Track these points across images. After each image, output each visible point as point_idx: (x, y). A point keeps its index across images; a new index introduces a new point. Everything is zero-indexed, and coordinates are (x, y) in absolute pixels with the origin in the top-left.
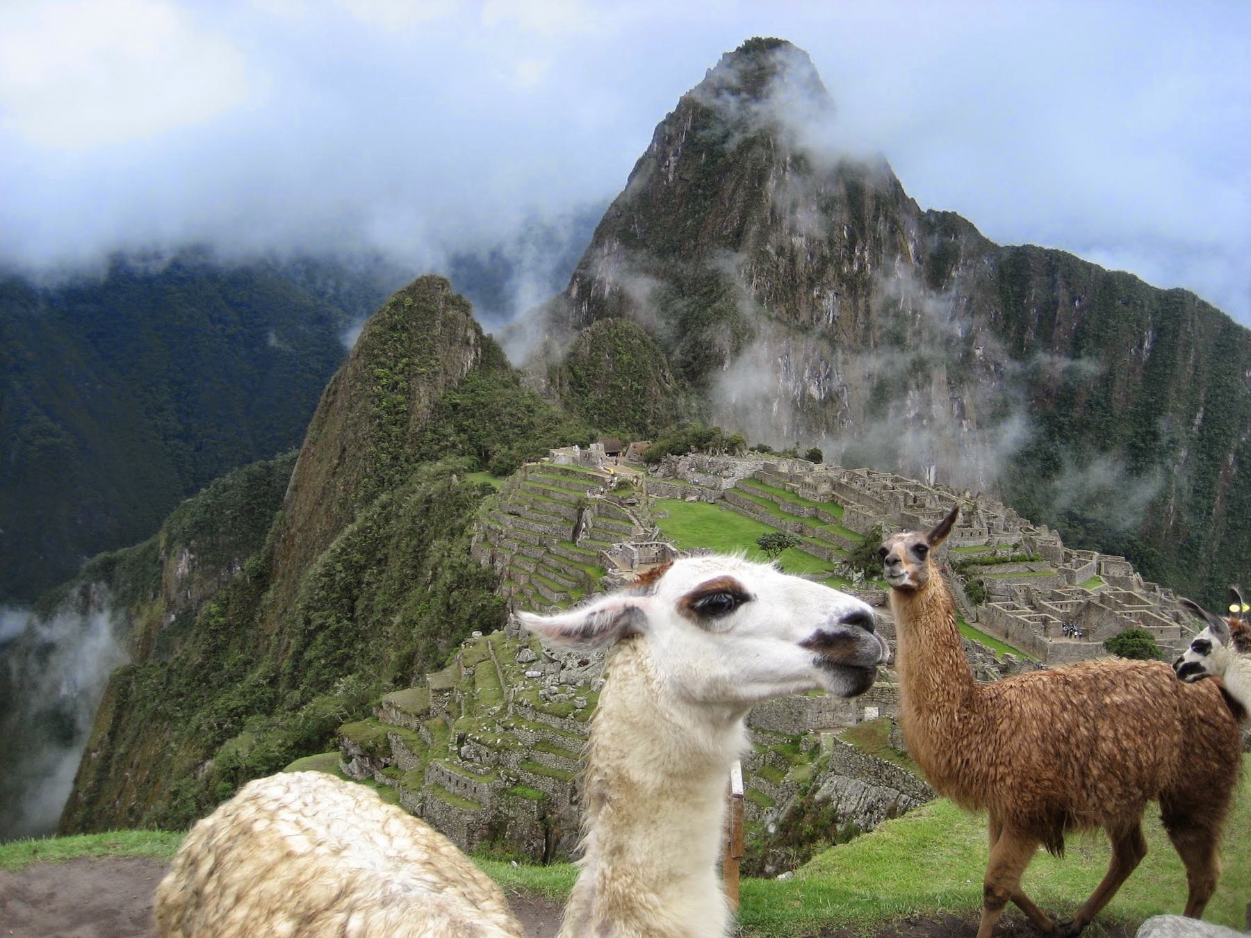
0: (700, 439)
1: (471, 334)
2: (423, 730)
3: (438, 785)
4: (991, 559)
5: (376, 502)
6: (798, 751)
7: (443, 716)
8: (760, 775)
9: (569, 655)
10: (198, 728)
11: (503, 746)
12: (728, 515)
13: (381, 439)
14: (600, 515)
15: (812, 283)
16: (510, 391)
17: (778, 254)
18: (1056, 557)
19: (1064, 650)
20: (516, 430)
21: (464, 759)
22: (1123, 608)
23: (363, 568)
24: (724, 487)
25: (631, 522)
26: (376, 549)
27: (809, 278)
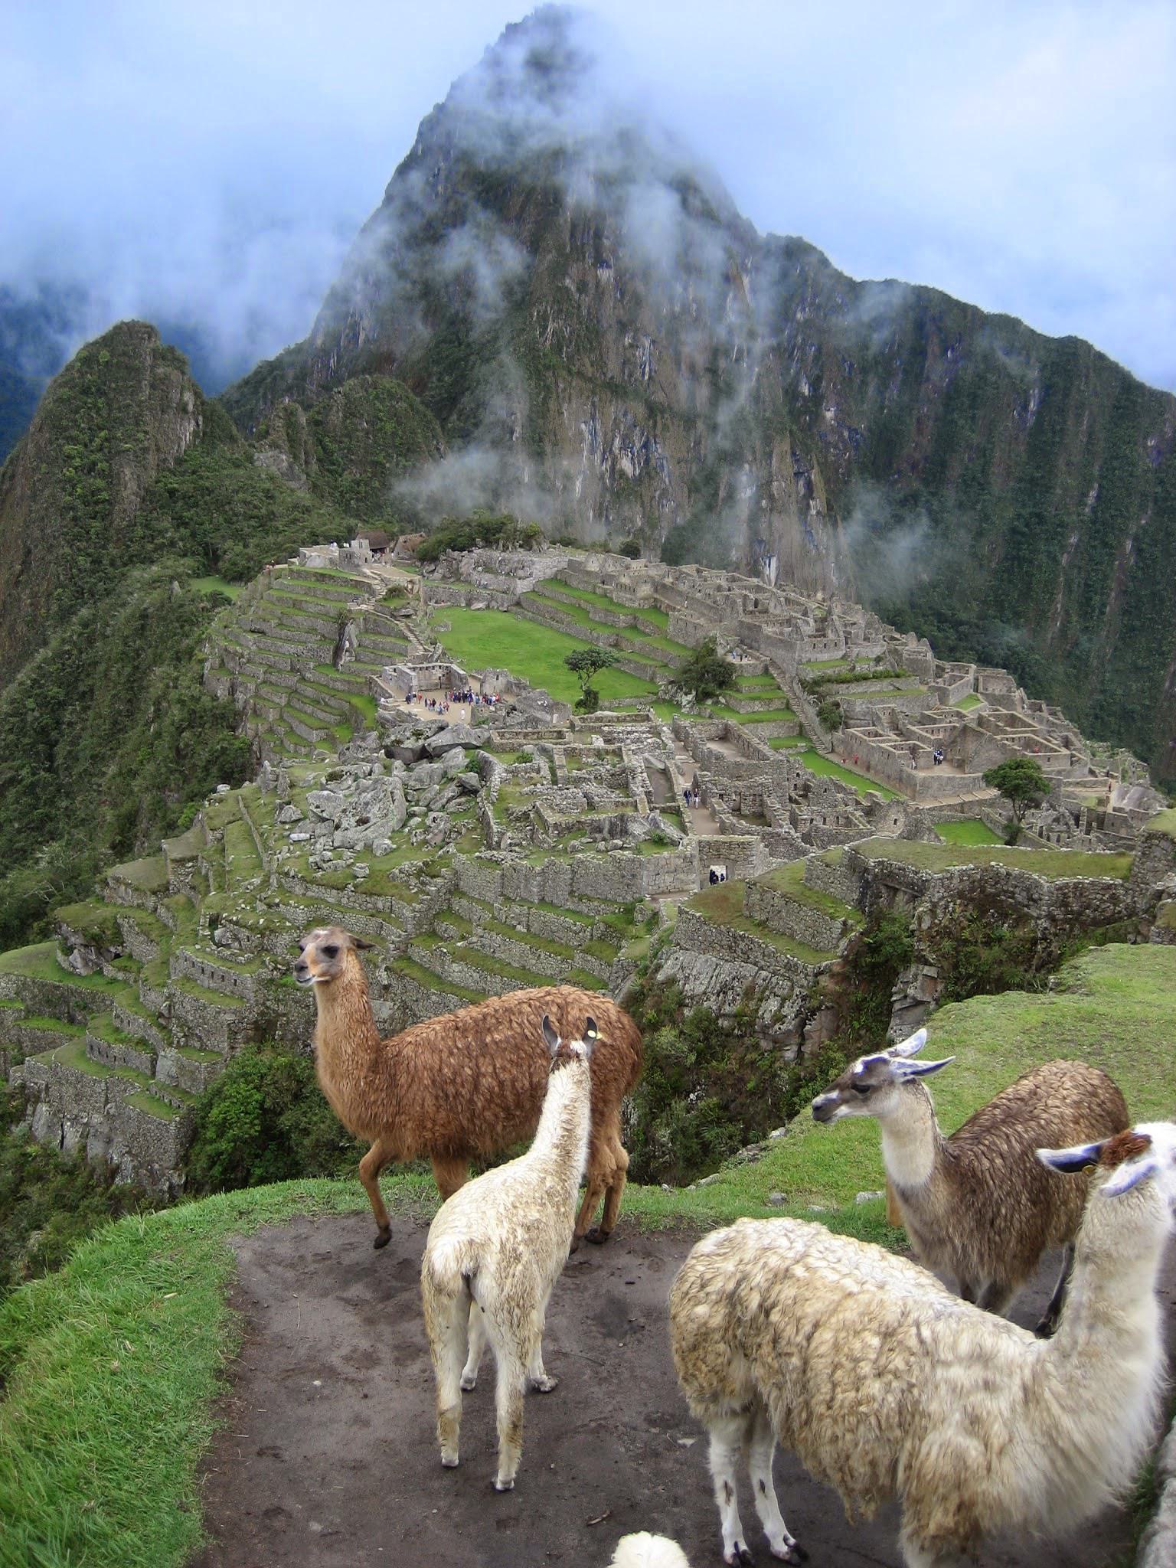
0: (488, 530)
1: (188, 397)
2: (162, 911)
3: (188, 978)
4: (849, 676)
5: (74, 619)
6: (631, 922)
7: (185, 891)
8: (587, 951)
9: (344, 811)
12: (526, 626)
13: (78, 537)
14: (367, 631)
16: (242, 472)
17: (578, 290)
18: (926, 671)
19: (936, 785)
20: (253, 523)
21: (218, 945)
22: (1005, 732)
23: (62, 704)
24: (519, 591)
25: (406, 638)
26: (77, 680)
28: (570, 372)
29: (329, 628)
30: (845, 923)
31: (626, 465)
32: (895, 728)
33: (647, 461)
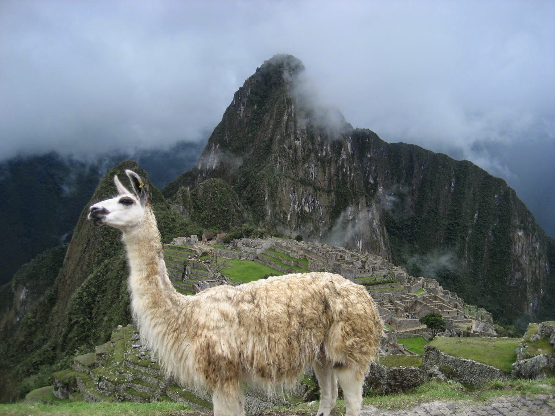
0: (248, 232)
2: (91, 374)
4: (373, 282)
5: (102, 264)
10: (18, 372)
11: (117, 382)
12: (259, 266)
13: (106, 235)
14: (194, 268)
15: (304, 161)
16: (164, 212)
17: (289, 148)
18: (404, 280)
19: (405, 323)
20: (167, 230)
22: (431, 302)
23: (96, 295)
24: (257, 253)
25: (208, 271)
26: (101, 286)
27: (303, 159)
28: (286, 177)
29: (181, 267)
30: (307, 386)
31: (307, 209)
32: (391, 302)
33: (314, 207)
